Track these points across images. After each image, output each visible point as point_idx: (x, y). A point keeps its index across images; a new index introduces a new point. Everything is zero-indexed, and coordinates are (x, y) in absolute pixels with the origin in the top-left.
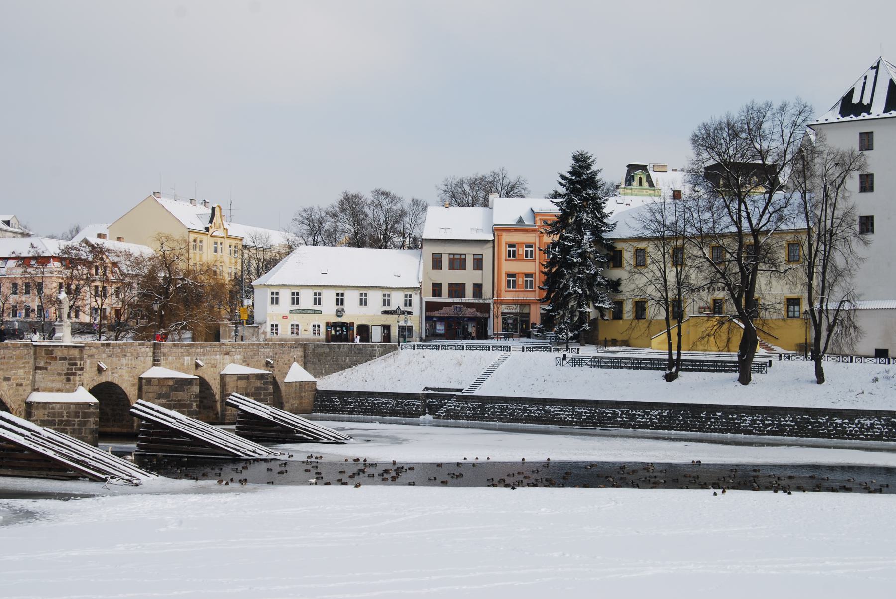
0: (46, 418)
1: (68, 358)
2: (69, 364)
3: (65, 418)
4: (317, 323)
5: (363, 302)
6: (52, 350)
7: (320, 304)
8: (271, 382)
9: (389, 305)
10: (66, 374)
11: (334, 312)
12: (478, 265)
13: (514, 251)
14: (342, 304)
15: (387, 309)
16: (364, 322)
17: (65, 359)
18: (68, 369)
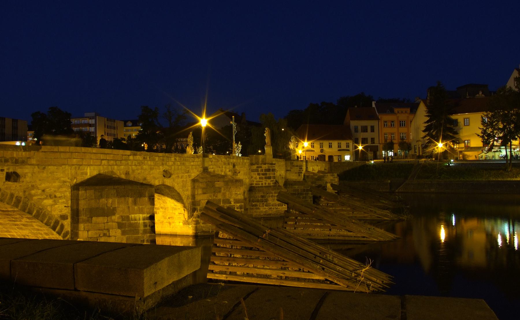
0: (292, 192)
1: (299, 165)
2: (299, 168)
3: (300, 192)
4: (312, 155)
5: (330, 146)
6: (293, 162)
7: (313, 147)
8: (336, 177)
9: (340, 147)
10: (299, 173)
11: (320, 151)
12: (373, 130)
13: (387, 124)
14: (322, 148)
15: (340, 149)
16: (330, 154)
17: (297, 166)
18: (299, 170)
